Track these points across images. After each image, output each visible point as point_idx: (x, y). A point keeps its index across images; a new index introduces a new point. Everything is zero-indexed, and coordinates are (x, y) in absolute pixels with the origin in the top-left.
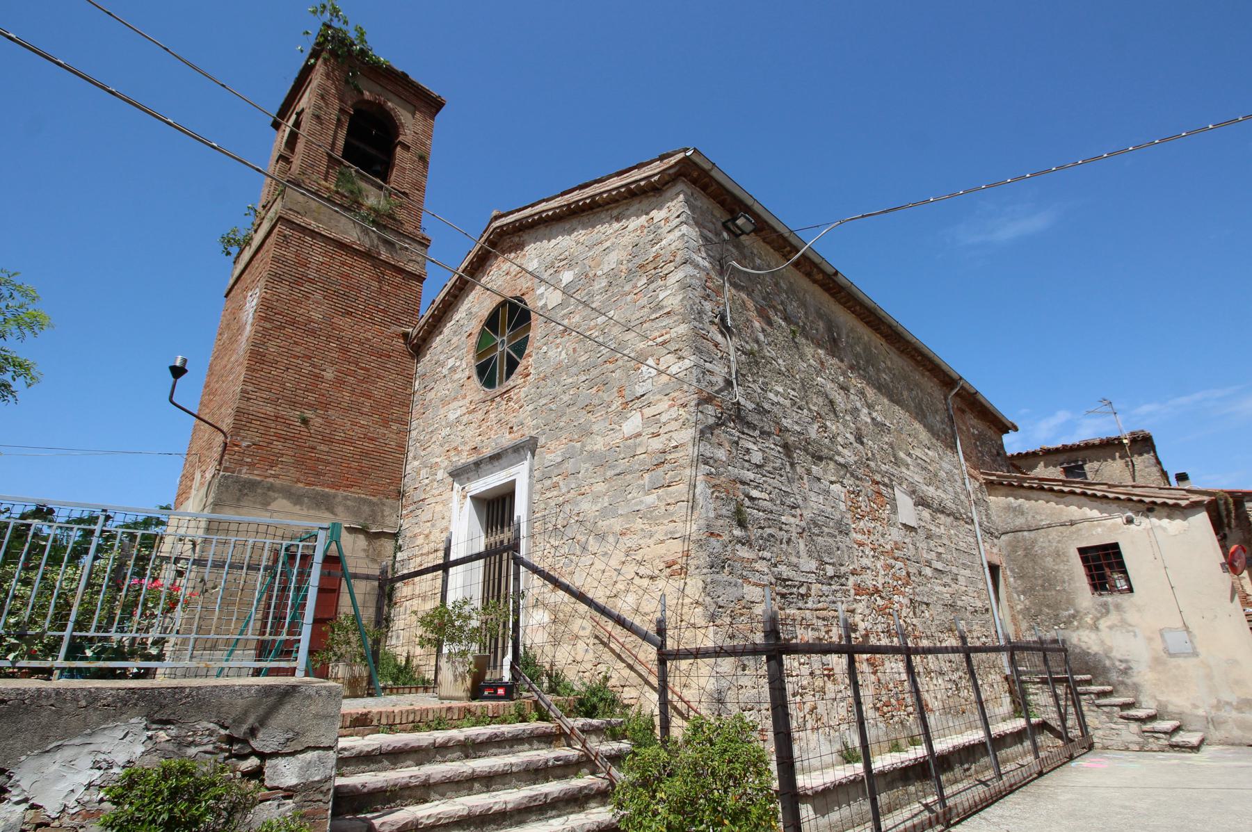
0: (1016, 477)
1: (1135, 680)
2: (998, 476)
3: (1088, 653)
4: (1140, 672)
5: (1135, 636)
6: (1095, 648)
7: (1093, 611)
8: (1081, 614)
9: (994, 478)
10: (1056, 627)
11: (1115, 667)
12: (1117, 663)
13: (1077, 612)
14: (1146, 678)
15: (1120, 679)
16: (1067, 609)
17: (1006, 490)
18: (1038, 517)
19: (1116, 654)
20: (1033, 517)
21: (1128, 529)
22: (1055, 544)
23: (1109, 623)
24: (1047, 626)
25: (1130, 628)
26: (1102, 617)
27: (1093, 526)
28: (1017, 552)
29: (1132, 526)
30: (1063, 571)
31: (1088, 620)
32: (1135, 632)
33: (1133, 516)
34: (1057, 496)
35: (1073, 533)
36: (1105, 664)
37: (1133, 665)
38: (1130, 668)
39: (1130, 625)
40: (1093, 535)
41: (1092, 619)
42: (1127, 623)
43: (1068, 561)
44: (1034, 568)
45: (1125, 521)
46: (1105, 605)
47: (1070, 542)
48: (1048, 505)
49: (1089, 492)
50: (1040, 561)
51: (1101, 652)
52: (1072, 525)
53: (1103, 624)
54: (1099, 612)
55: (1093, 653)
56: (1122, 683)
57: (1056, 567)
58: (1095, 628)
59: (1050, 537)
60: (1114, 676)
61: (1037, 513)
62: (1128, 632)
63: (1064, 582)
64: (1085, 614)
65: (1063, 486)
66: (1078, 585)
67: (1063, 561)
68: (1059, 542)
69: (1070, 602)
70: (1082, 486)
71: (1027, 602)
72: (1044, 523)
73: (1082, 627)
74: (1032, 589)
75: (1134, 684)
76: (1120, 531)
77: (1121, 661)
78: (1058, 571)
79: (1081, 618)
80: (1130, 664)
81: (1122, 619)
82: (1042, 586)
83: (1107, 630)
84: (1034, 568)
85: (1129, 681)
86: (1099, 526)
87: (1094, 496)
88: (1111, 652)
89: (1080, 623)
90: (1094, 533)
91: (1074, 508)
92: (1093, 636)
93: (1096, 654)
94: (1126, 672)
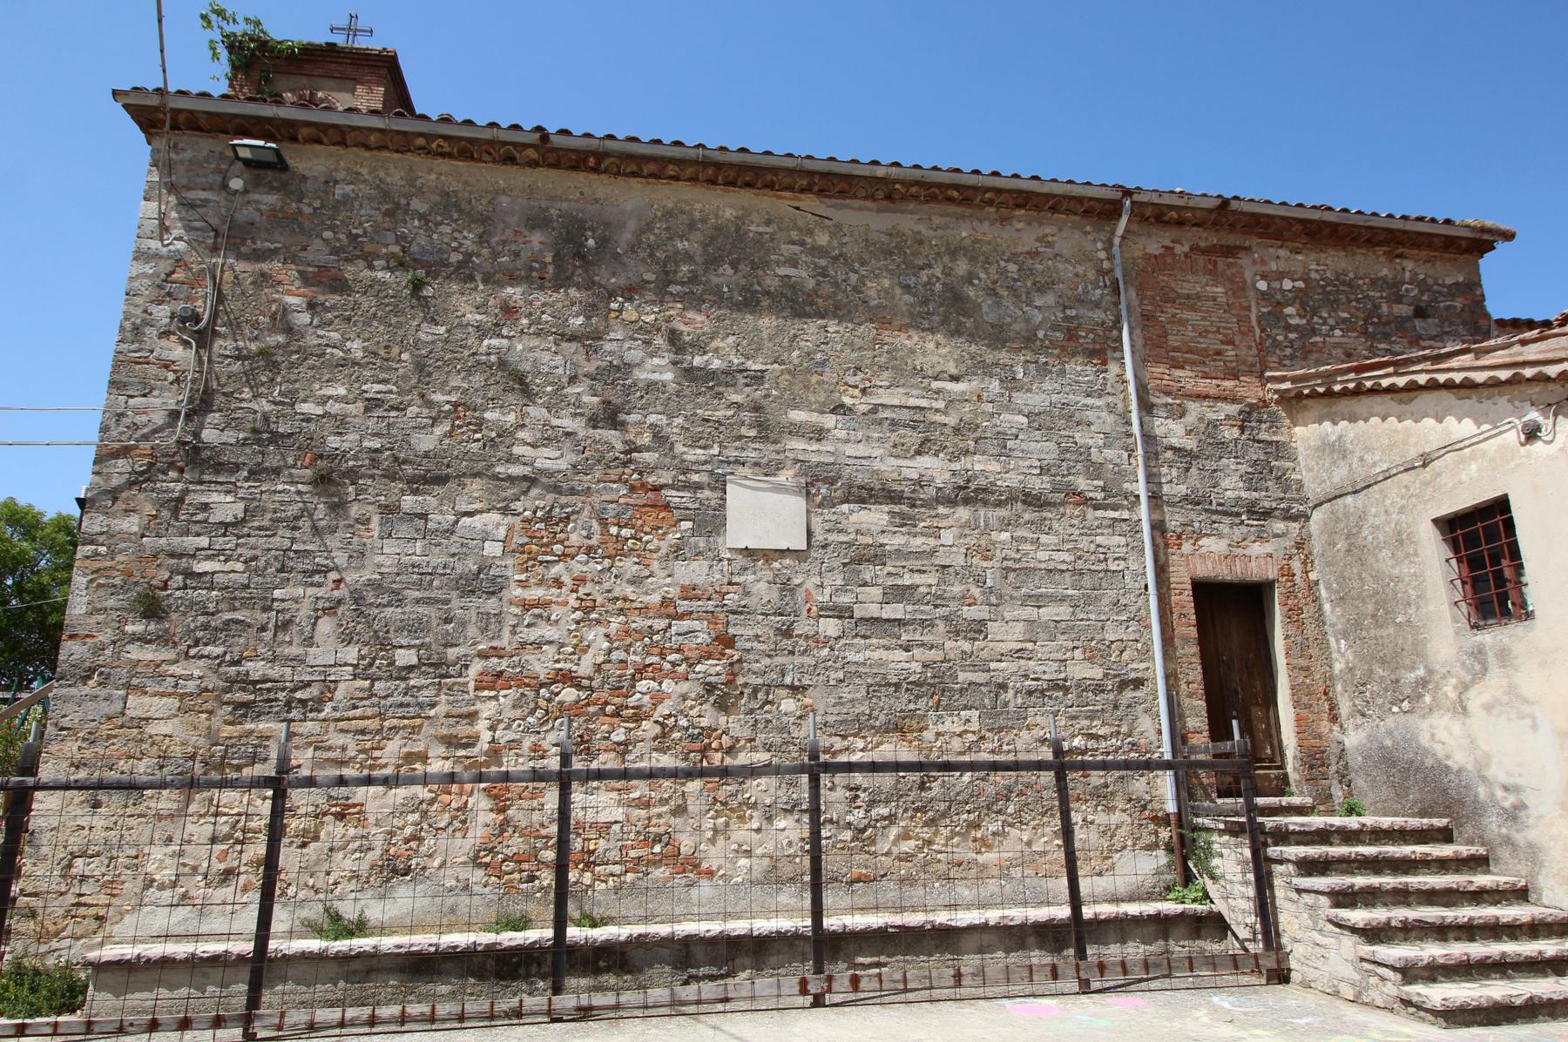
0: (1317, 375)
1: (1532, 835)
2: (1294, 380)
3: (1447, 767)
4: (1539, 818)
5: (1534, 727)
6: (1459, 759)
7: (1458, 669)
8: (1437, 677)
9: (1287, 385)
10: (1395, 709)
11: (1496, 804)
12: (1499, 793)
13: (1430, 672)
14: (1554, 831)
15: (1504, 831)
16: (1413, 668)
17: (1316, 407)
18: (1369, 458)
19: (1497, 773)
20: (1361, 459)
21: (1528, 455)
22: (1394, 517)
23: (1485, 698)
24: (1381, 706)
25: (1526, 709)
26: (1473, 681)
27: (1462, 461)
28: (1335, 544)
29: (1538, 446)
30: (1407, 579)
31: (1449, 690)
32: (1534, 719)
33: (1540, 419)
34: (1401, 402)
35: (1426, 484)
36: (1476, 796)
37: (1529, 799)
38: (1523, 806)
39: (1526, 701)
40: (1460, 482)
41: (1455, 687)
42: (1517, 696)
43: (1416, 554)
44: (1361, 578)
45: (1523, 437)
46: (1478, 653)
47: (1420, 507)
48: (1386, 425)
49: (1441, 378)
50: (1371, 560)
51: (1470, 767)
52: (1424, 465)
53: (1477, 698)
54: (1468, 671)
55: (1455, 767)
56: (1508, 841)
57: (1396, 572)
58: (1462, 709)
59: (1388, 502)
60: (1493, 825)
61: (1367, 449)
62: (1522, 717)
63: (1409, 604)
64: (1444, 677)
65: (1396, 374)
66: (1431, 608)
67: (1408, 555)
68: (1402, 510)
69: (1419, 650)
70: (1427, 365)
71: (1350, 655)
72: (1378, 470)
73: (1439, 707)
74: (1358, 624)
75: (1530, 845)
76: (1513, 464)
77: (1506, 788)
78: (1398, 579)
79: (1437, 688)
80: (1523, 797)
81: (1509, 685)
82: (1374, 616)
83: (1483, 713)
84: (1361, 578)
85: (1520, 838)
86: (1473, 458)
87: (1468, 385)
88: (1488, 765)
89: (1434, 698)
90: (1464, 477)
91: (1429, 422)
92: (1456, 727)
93: (1460, 771)
94: (1513, 815)
